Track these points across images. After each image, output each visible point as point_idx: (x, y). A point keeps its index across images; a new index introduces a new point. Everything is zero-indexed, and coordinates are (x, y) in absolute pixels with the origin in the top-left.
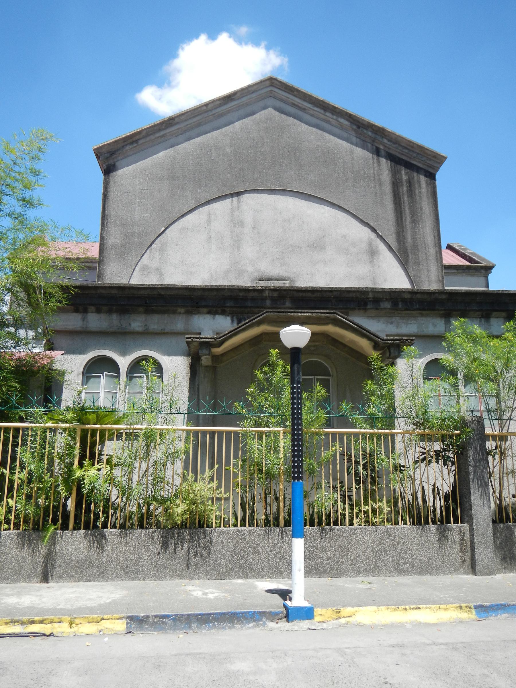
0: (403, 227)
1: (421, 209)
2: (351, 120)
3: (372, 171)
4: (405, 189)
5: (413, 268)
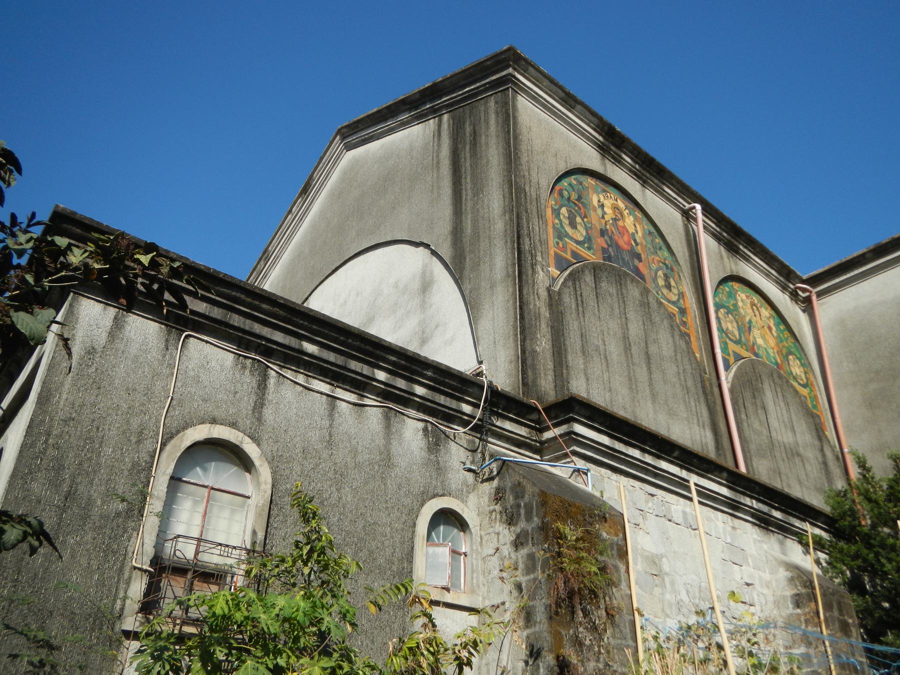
0: (461, 213)
1: (488, 162)
3: (431, 158)
4: (468, 147)
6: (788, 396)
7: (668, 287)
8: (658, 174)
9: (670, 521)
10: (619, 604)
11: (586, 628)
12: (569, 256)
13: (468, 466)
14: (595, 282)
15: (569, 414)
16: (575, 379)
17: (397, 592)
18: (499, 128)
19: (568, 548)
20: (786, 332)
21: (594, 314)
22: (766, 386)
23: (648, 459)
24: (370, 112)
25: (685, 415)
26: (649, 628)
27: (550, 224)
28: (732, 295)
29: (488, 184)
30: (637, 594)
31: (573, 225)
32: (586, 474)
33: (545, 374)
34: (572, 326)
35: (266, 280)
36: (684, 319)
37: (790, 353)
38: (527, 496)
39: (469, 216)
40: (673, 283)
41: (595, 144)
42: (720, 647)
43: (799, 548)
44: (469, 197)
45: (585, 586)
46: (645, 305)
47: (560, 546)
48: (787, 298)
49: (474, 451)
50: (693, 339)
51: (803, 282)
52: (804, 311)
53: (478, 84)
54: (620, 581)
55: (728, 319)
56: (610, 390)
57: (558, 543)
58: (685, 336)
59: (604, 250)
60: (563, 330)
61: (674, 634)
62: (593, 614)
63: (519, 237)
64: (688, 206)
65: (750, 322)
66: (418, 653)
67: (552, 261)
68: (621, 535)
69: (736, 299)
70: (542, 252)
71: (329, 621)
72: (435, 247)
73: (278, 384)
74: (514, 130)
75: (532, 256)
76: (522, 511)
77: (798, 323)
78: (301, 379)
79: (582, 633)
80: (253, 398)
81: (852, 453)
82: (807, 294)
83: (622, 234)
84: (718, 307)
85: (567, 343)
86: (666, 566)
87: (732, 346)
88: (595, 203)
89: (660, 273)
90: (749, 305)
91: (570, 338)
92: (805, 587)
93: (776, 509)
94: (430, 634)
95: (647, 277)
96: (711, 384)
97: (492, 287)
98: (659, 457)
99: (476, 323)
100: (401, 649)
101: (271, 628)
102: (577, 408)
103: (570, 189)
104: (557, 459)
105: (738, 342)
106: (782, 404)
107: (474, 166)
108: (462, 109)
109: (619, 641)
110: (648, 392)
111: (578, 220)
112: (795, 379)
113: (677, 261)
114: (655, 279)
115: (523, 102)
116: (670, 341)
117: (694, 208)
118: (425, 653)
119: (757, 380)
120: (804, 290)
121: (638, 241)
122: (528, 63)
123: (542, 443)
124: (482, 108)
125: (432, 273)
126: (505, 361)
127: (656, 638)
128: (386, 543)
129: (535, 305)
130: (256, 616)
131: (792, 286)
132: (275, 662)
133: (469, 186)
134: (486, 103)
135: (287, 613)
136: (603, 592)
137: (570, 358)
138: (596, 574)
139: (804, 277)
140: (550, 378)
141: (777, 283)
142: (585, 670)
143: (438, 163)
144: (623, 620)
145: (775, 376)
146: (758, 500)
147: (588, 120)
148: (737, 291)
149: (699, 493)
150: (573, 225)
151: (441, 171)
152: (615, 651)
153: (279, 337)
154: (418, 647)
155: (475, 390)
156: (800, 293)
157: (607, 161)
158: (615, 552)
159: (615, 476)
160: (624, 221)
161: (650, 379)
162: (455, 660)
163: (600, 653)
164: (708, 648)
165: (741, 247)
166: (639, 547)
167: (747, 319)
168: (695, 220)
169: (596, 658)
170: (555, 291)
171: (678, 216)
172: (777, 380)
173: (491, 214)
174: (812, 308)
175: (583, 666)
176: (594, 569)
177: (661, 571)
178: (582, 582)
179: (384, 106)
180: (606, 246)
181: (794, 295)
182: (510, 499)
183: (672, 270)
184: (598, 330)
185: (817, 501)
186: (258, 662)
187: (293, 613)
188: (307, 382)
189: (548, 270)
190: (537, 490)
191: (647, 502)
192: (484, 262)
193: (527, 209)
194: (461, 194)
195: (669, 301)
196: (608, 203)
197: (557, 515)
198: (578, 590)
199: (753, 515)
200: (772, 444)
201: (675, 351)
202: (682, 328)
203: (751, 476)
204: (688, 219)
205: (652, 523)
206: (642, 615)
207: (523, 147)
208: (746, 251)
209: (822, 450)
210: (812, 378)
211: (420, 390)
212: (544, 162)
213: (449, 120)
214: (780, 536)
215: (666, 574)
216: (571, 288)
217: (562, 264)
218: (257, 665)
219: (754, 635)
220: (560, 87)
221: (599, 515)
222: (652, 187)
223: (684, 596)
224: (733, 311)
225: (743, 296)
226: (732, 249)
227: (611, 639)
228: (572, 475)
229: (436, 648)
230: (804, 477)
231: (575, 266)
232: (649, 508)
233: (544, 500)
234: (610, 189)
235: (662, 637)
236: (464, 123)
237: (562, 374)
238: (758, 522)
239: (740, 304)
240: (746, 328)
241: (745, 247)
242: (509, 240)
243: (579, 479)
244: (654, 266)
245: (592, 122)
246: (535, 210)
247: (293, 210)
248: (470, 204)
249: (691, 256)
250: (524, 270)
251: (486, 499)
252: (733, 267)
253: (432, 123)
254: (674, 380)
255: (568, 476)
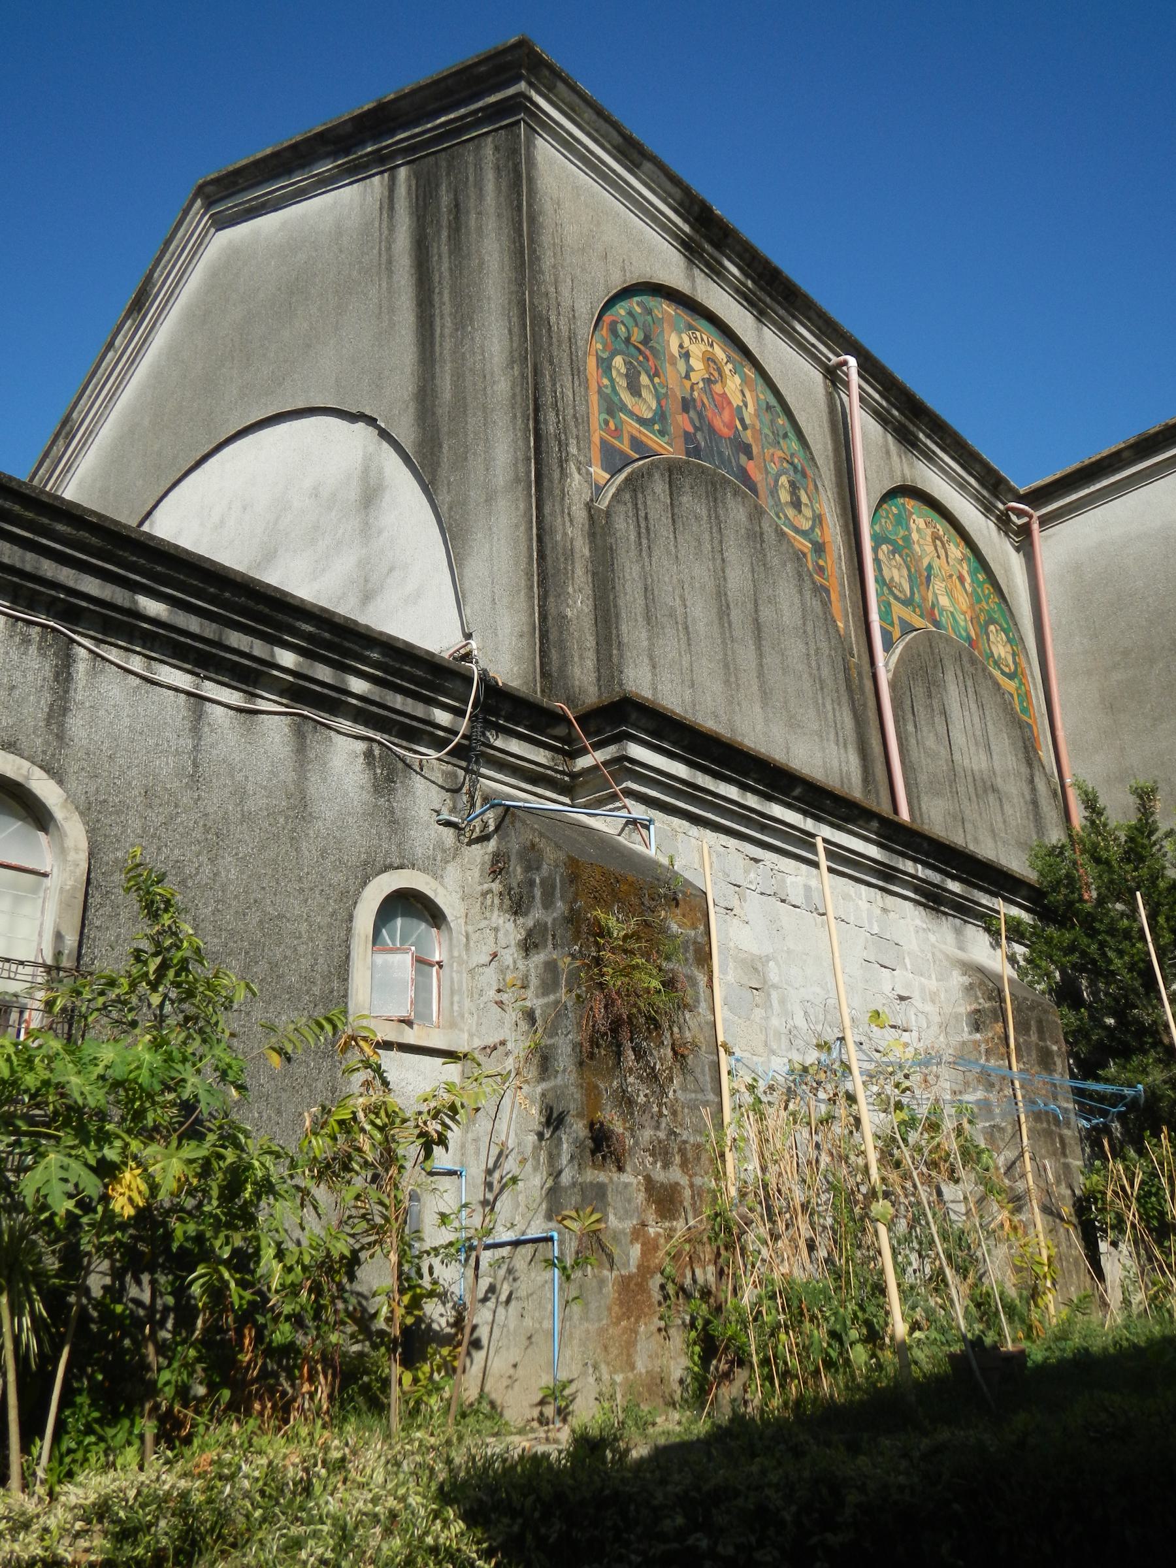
0: (433, 361)
1: (481, 264)
2: (330, 148)
3: (375, 251)
4: (444, 234)
5: (449, 484)
6: (984, 693)
7: (797, 504)
8: (785, 298)
9: (783, 901)
10: (694, 1037)
11: (640, 1077)
12: (625, 447)
13: (445, 816)
14: (671, 494)
15: (619, 726)
16: (632, 666)
17: (317, 1030)
18: (502, 199)
19: (613, 950)
20: (987, 585)
21: (668, 552)
22: (950, 676)
23: (752, 801)
24: (259, 155)
25: (816, 727)
26: (741, 1073)
27: (594, 386)
28: (902, 520)
29: (481, 307)
30: (724, 1020)
31: (635, 389)
32: (647, 828)
33: (581, 657)
34: (630, 572)
35: (69, 475)
36: (821, 562)
37: (992, 621)
38: (545, 866)
39: (448, 367)
40: (804, 498)
41: (676, 237)
42: (851, 1098)
43: (984, 939)
44: (447, 331)
45: (639, 1011)
46: (755, 537)
47: (599, 948)
48: (992, 525)
49: (456, 791)
50: (833, 597)
51: (1021, 499)
52: (1018, 550)
53: (462, 111)
54: (697, 1001)
55: (894, 563)
56: (692, 686)
57: (597, 943)
58: (821, 591)
59: (688, 438)
60: (613, 580)
61: (781, 1079)
62: (651, 1054)
63: (537, 410)
64: (835, 360)
65: (930, 567)
66: (356, 1128)
67: (596, 454)
68: (702, 927)
69: (908, 528)
70: (577, 437)
71: (193, 1085)
72: (387, 423)
73: (93, 673)
74: (530, 205)
75: (560, 442)
76: (538, 893)
77: (1008, 570)
78: (136, 663)
79: (632, 1085)
80: (47, 698)
81: (1078, 786)
82: (1025, 520)
83: (720, 408)
84: (878, 540)
85: (621, 602)
86: (773, 973)
87: (898, 610)
88: (674, 349)
89: (783, 480)
90: (929, 539)
91: (626, 594)
92: (990, 999)
93: (954, 878)
94: (375, 1097)
95: (762, 488)
96: (860, 674)
97: (489, 500)
98: (769, 798)
99: (461, 566)
100: (325, 1123)
101: (89, 1098)
102: (634, 716)
103: (629, 322)
104: (600, 803)
105: (907, 602)
106: (973, 706)
107: (457, 270)
108: (432, 159)
109: (693, 1095)
110: (755, 687)
111: (644, 379)
112: (997, 664)
113: (813, 459)
114: (774, 492)
115: (545, 150)
116: (797, 601)
117: (845, 363)
118: (368, 1127)
119: (935, 667)
120: (1020, 513)
121: (748, 421)
122: (556, 74)
123: (573, 776)
124: (471, 159)
125: (380, 471)
126: (512, 634)
127: (751, 1088)
128: (302, 949)
129: (565, 534)
130: (62, 1079)
131: (1001, 506)
132: (99, 1155)
133: (447, 309)
134: (478, 148)
135: (118, 1073)
136: (669, 1020)
137: (624, 628)
138: (660, 991)
139: (1022, 491)
140: (590, 664)
141: (977, 500)
142: (637, 1143)
143: (390, 262)
144: (699, 1062)
145: (965, 659)
146: (926, 865)
147: (665, 192)
148: (911, 513)
149: (830, 855)
150: (634, 388)
151: (395, 278)
152: (686, 1110)
153: (91, 586)
154: (355, 1119)
155: (456, 686)
156: (1014, 518)
157: (697, 272)
158: (690, 955)
159: (694, 831)
160: (724, 385)
161: (761, 665)
162: (419, 1137)
163: (661, 1114)
164: (832, 1101)
165: (921, 436)
166: (732, 945)
167: (925, 563)
168: (847, 385)
169: (654, 1123)
170: (600, 510)
171: (816, 377)
172: (967, 666)
173: (488, 366)
174: (1032, 544)
175: (633, 1137)
176: (655, 984)
177: (765, 982)
178: (635, 1005)
179: (286, 144)
180: (691, 430)
181: (1003, 522)
182: (518, 872)
183: (804, 475)
184: (675, 580)
185: (1018, 864)
186: (70, 1156)
187: (131, 1072)
188: (149, 669)
189: (589, 473)
190: (562, 856)
191: (747, 872)
192: (475, 454)
193: (551, 356)
194: (432, 324)
195: (797, 530)
196: (696, 350)
197: (595, 897)
198: (628, 1017)
199: (916, 890)
200: (953, 773)
201: (804, 617)
202: (816, 577)
203: (915, 827)
204: (834, 384)
205: (753, 906)
206: (730, 1053)
207: (546, 239)
208: (929, 442)
209: (1031, 781)
210: (1024, 664)
211: (358, 685)
212: (583, 270)
213: (408, 179)
214: (958, 921)
215: (775, 987)
216: (629, 505)
217: (613, 461)
218: (66, 1160)
219: (907, 1076)
220: (615, 125)
221: (665, 896)
222: (774, 323)
223: (799, 1020)
224: (902, 548)
225: (920, 522)
226: (906, 439)
227: (679, 1092)
228: (623, 830)
229: (386, 1120)
230: (1001, 825)
231: (636, 465)
232: (751, 882)
233: (574, 871)
234: (703, 324)
235: (762, 1086)
236: (438, 186)
237: (611, 656)
238: (923, 900)
239: (915, 536)
240: (923, 578)
241: (928, 436)
242: (519, 415)
243: (636, 837)
244: (773, 468)
245: (670, 195)
246: (565, 356)
247: (117, 343)
248: (448, 345)
249: (836, 450)
250: (545, 470)
251: (477, 875)
252: (907, 472)
253: (377, 183)
254: (800, 667)
255: (617, 832)
